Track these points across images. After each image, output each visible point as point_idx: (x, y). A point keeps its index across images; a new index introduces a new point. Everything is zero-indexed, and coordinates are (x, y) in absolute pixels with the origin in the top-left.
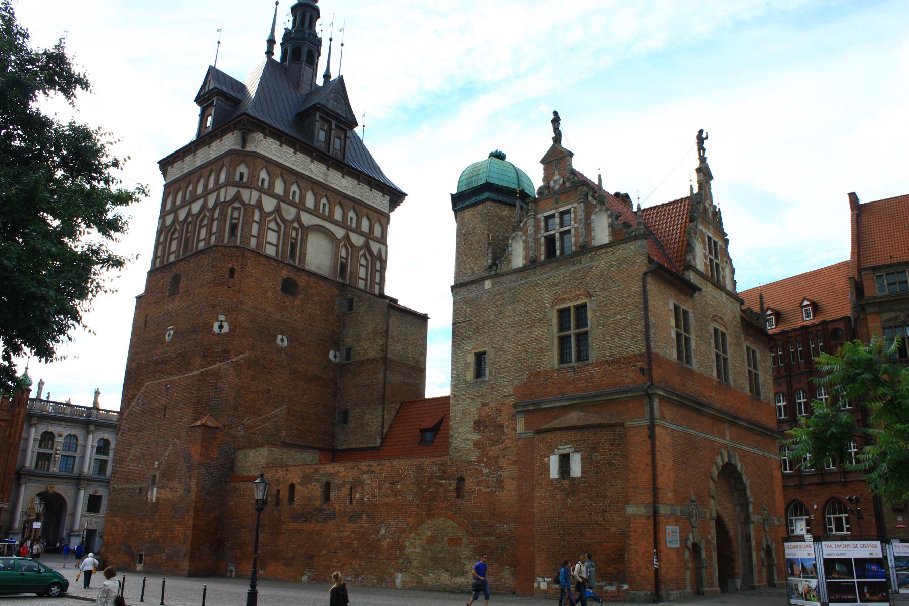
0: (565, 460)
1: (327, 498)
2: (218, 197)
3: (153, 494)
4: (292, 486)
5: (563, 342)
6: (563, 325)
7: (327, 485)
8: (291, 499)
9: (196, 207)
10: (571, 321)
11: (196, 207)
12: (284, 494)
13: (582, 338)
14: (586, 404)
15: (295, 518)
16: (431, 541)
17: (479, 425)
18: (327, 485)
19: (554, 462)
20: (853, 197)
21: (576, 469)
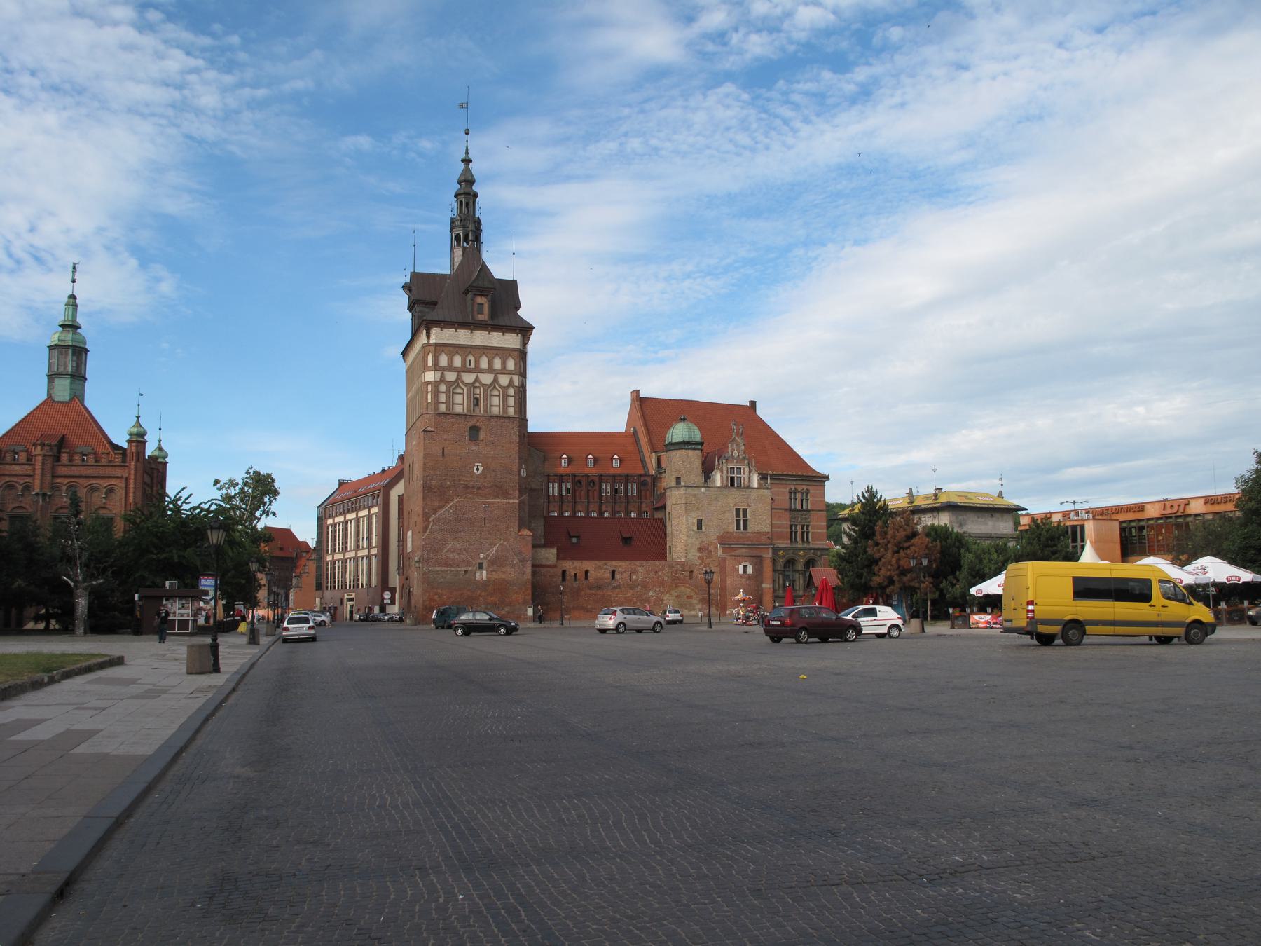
0: (745, 567)
1: (613, 577)
2: (511, 380)
3: (483, 575)
4: (587, 572)
5: (738, 522)
6: (738, 515)
7: (613, 572)
8: (587, 577)
9: (487, 379)
10: (741, 514)
11: (487, 379)
12: (581, 575)
13: (745, 522)
14: (750, 547)
15: (590, 587)
16: (678, 597)
17: (699, 550)
18: (613, 572)
19: (741, 568)
20: (638, 391)
21: (750, 570)
